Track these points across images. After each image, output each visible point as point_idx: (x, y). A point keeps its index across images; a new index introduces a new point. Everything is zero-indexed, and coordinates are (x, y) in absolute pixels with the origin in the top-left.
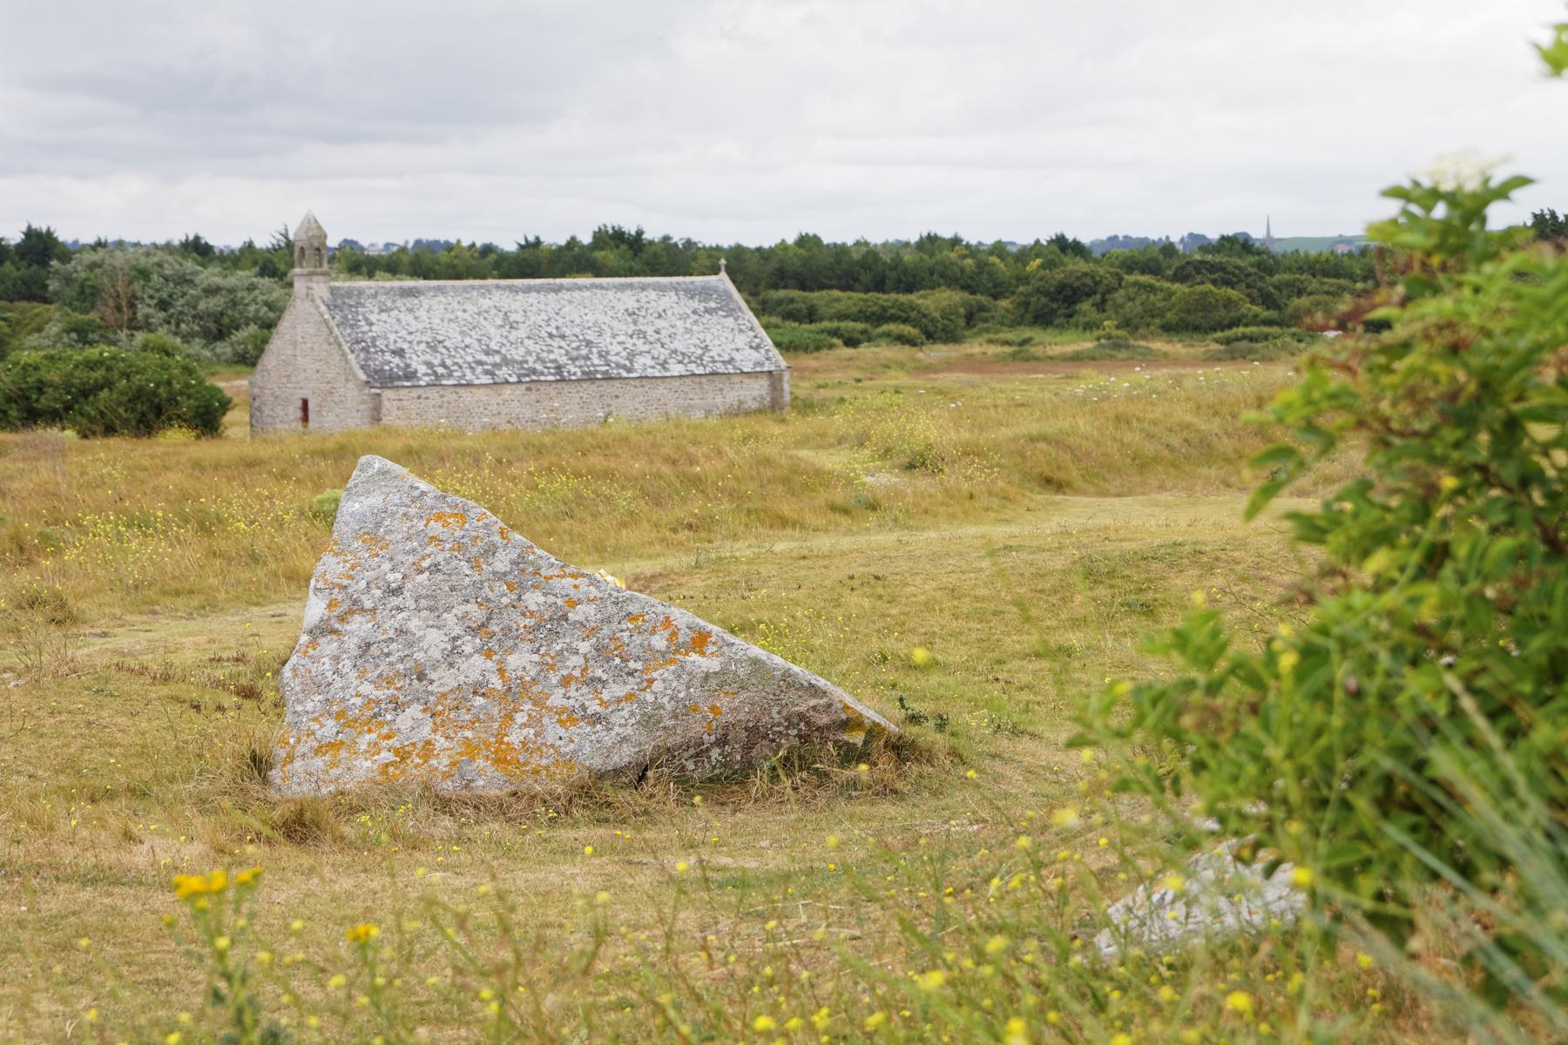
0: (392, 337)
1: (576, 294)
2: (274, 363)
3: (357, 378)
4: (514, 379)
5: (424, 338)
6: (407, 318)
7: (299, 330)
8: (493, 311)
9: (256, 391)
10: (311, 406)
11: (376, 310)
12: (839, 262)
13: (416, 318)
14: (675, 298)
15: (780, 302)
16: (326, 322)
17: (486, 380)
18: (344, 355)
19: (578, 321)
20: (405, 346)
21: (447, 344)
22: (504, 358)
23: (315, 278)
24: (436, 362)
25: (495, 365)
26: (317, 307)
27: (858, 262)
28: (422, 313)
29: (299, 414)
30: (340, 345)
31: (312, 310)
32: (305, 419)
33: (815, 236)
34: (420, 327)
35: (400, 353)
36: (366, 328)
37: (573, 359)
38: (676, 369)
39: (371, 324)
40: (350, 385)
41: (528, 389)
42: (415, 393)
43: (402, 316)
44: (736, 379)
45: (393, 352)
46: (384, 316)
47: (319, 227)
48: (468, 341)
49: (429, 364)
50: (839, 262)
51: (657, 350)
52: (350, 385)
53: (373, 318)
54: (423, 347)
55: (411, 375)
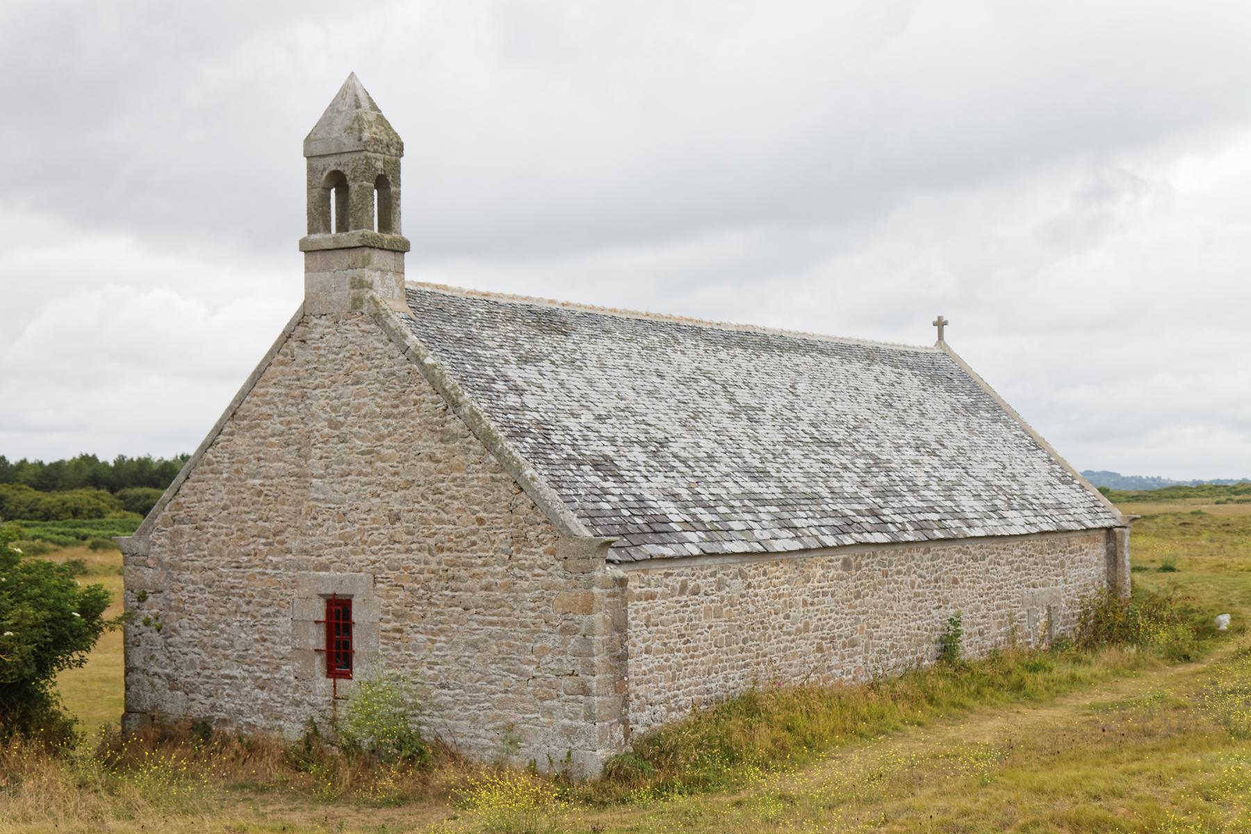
0: (571, 423)
1: (797, 359)
2: (222, 497)
3: (562, 532)
4: (830, 541)
5: (632, 433)
6: (575, 381)
7: (319, 402)
8: (705, 382)
9: (149, 575)
10: (359, 615)
11: (513, 359)
12: (141, 471)
13: (590, 382)
14: (916, 380)
15: (137, 498)
16: (430, 374)
17: (785, 542)
18: (505, 463)
19: (832, 413)
20: (609, 450)
21: (675, 448)
22: (786, 491)
23: (377, 257)
24: (684, 493)
25: (783, 504)
26: (395, 337)
27: (157, 472)
28: (593, 372)
29: (316, 639)
30: (489, 441)
31: (375, 343)
32: (339, 657)
33: (85, 458)
34: (611, 403)
35: (603, 465)
36: (512, 400)
37: (883, 493)
38: (1018, 523)
39: (520, 392)
40: (540, 555)
41: (846, 565)
42: (679, 575)
43: (563, 376)
44: (1076, 542)
45: (596, 466)
46: (531, 371)
47: (382, 121)
48: (707, 446)
49: (675, 497)
50: (141, 471)
51: (971, 483)
52: (540, 555)
53: (513, 372)
54: (637, 454)
55: (658, 528)
